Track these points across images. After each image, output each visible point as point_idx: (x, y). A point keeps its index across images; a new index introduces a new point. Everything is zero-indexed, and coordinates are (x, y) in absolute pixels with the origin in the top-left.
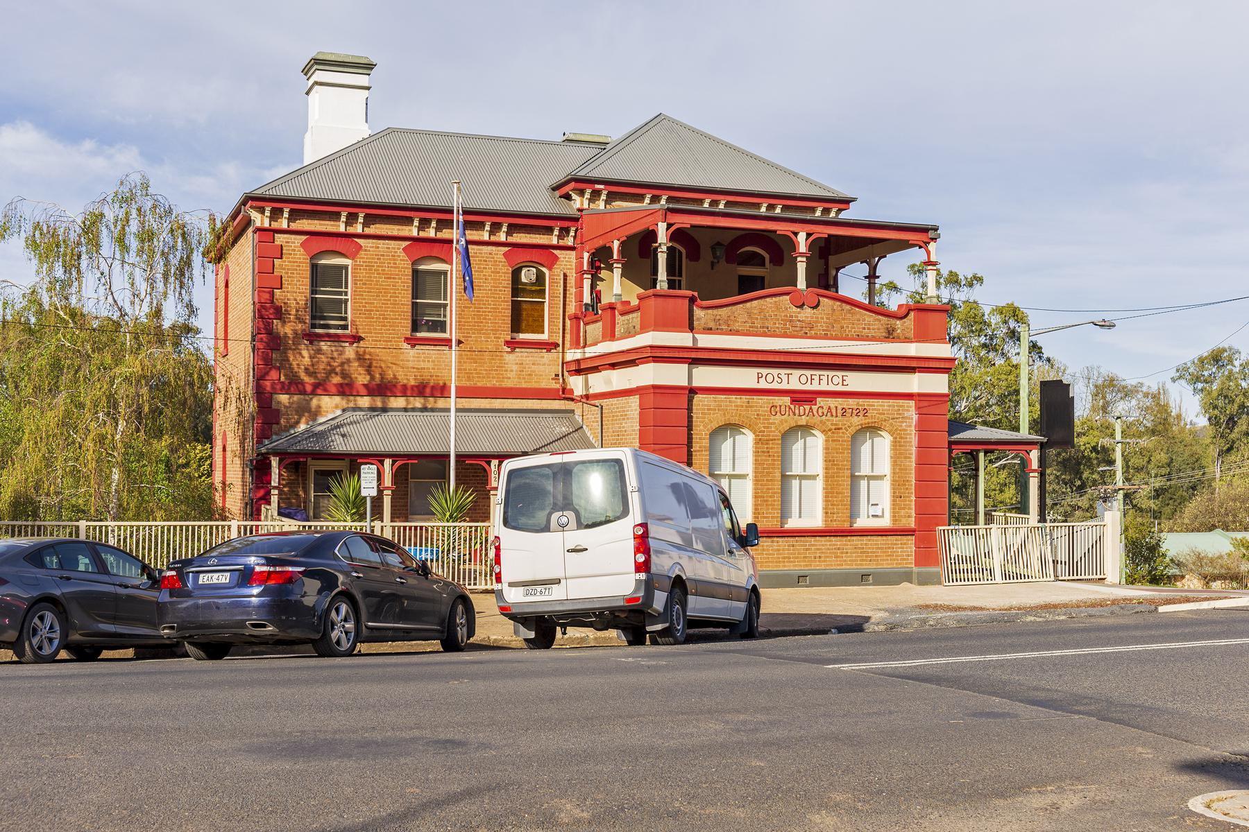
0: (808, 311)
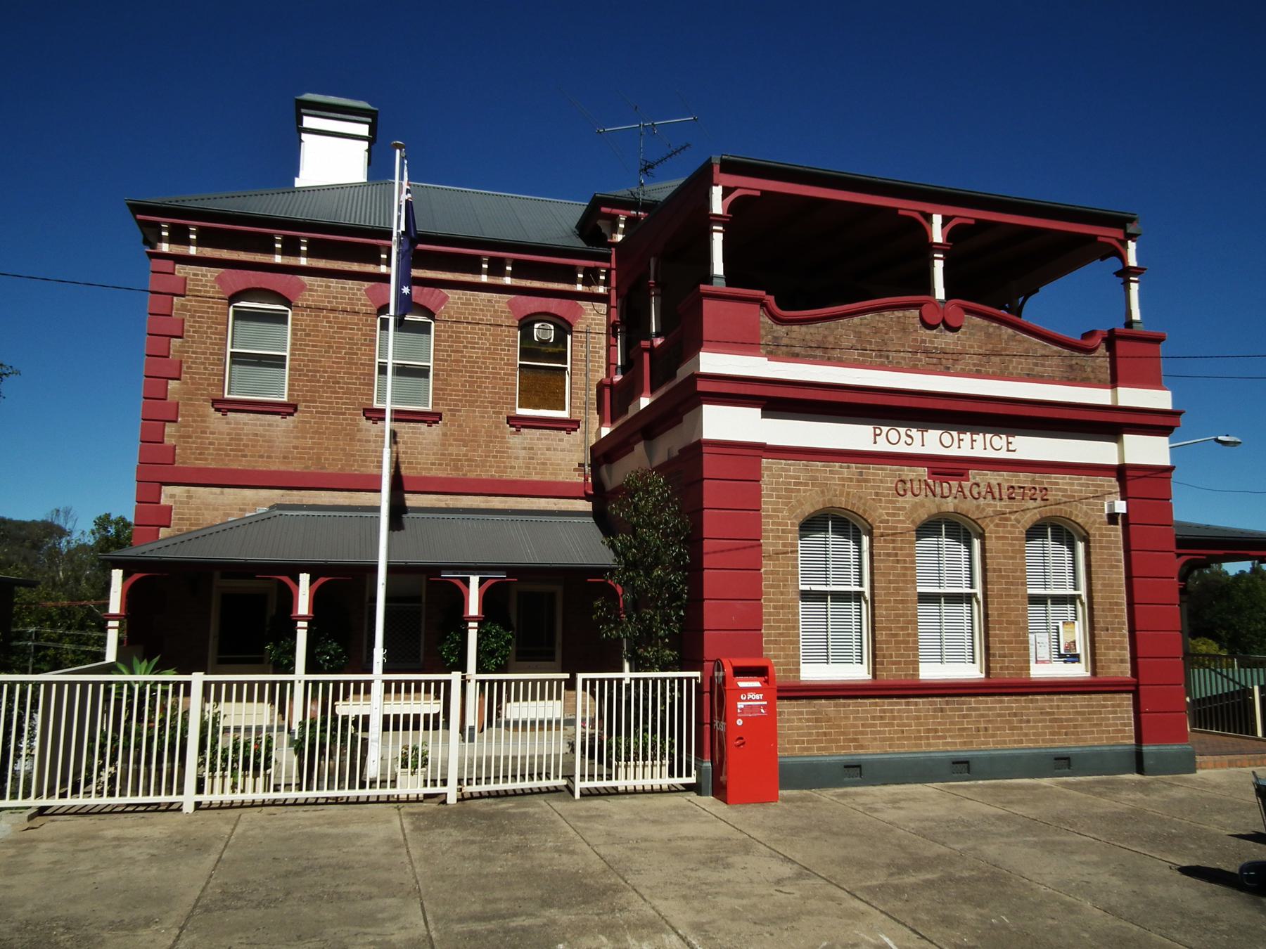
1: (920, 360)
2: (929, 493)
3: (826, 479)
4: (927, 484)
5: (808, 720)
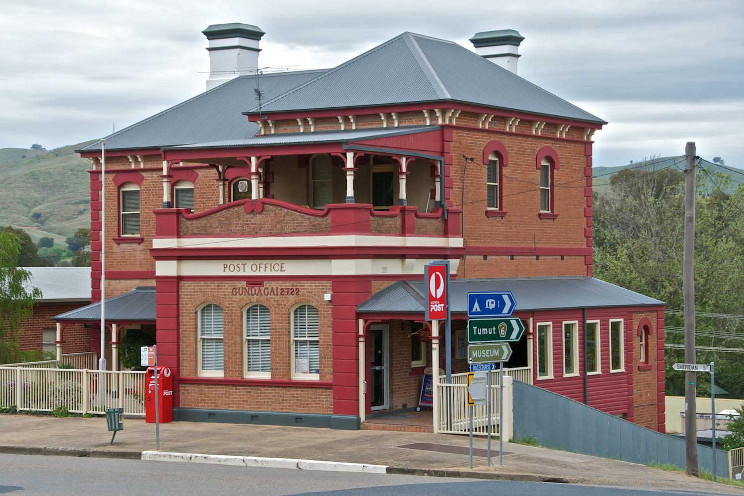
0: (259, 217)
1: (245, 230)
2: (246, 294)
3: (205, 289)
4: (245, 289)
5: (198, 394)
